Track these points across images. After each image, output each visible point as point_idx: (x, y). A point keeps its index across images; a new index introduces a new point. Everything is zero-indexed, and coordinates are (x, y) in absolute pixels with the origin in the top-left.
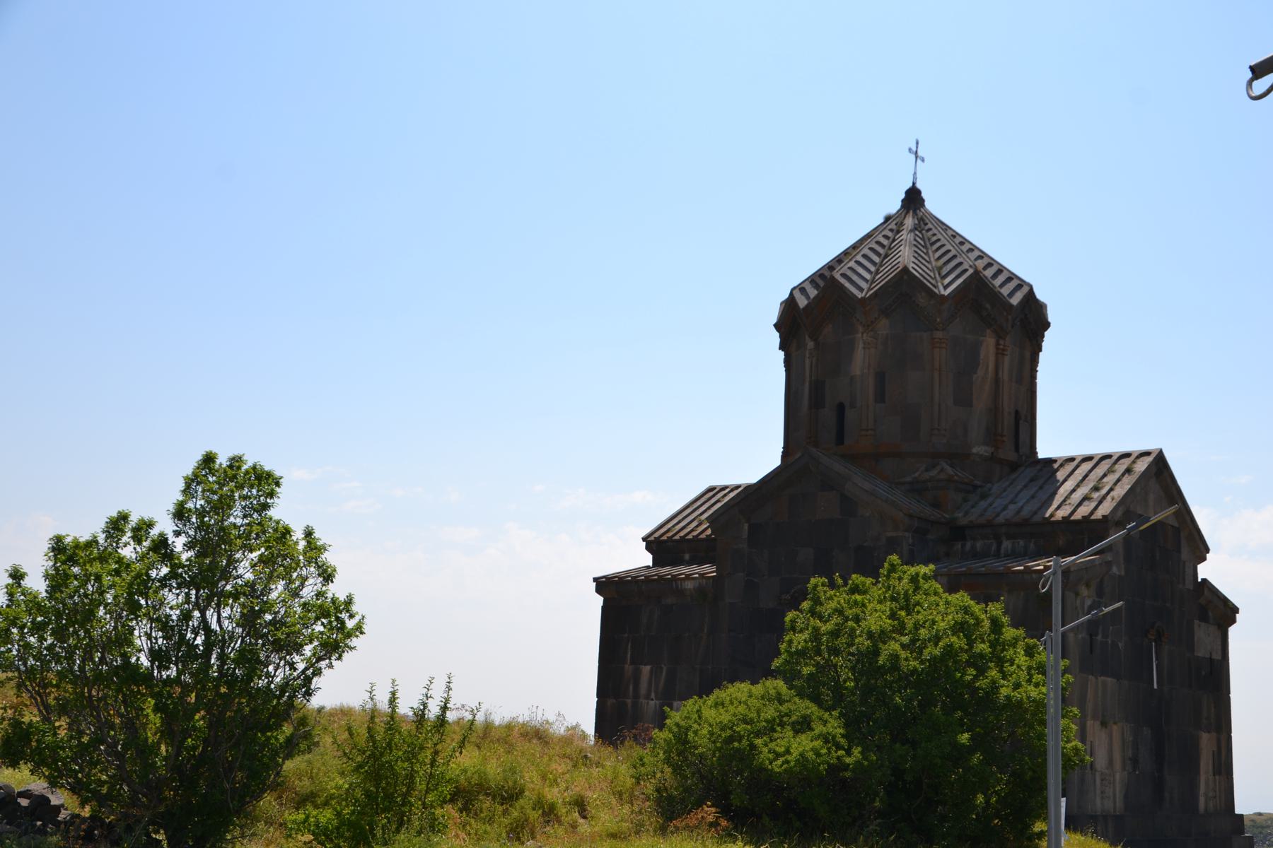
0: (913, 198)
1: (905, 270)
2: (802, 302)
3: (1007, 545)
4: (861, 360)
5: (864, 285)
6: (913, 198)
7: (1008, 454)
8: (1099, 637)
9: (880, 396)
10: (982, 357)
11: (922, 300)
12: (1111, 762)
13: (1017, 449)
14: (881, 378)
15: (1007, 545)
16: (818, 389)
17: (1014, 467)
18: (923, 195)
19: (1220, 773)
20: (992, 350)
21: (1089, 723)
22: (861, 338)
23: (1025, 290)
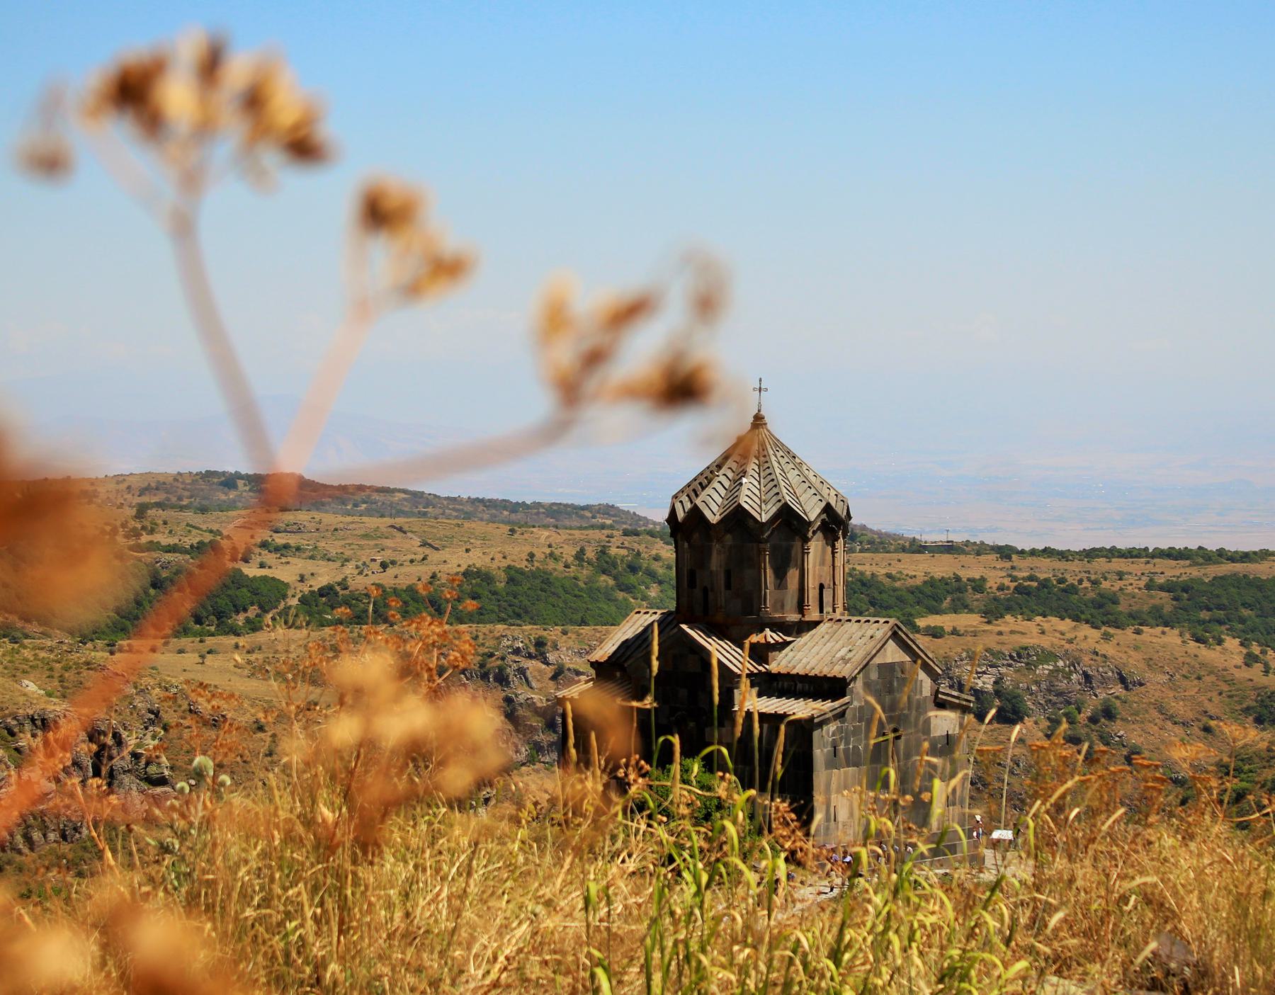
0: (758, 421)
1: (739, 505)
2: (681, 515)
3: (799, 686)
4: (716, 562)
5: (715, 508)
6: (758, 421)
7: (813, 615)
8: (842, 747)
9: (728, 586)
10: (793, 553)
11: (751, 523)
12: (851, 814)
13: (821, 611)
14: (728, 574)
15: (799, 686)
16: (692, 574)
17: (816, 624)
18: (767, 420)
19: (954, 804)
20: (800, 550)
21: (833, 796)
22: (716, 547)
23: (823, 504)
